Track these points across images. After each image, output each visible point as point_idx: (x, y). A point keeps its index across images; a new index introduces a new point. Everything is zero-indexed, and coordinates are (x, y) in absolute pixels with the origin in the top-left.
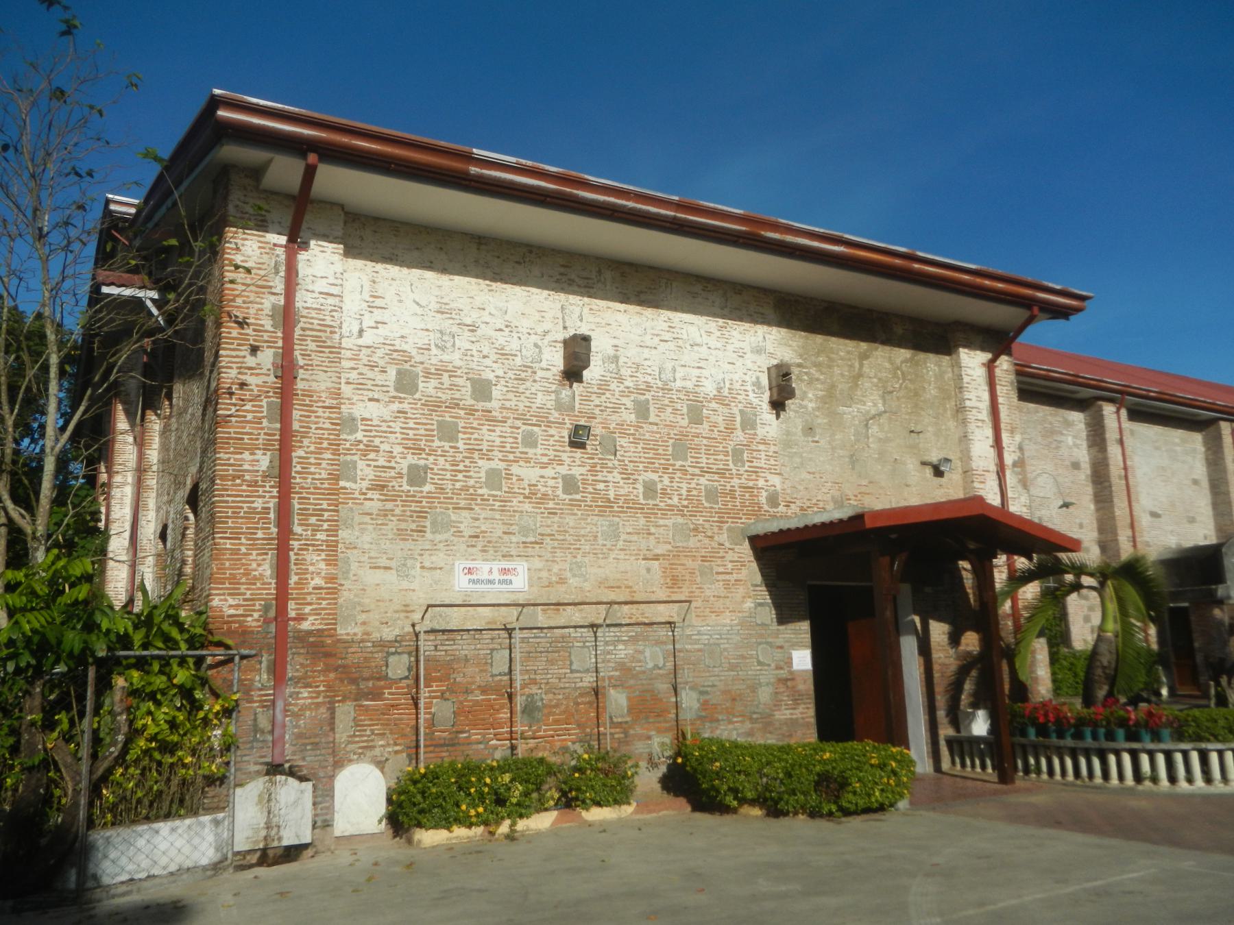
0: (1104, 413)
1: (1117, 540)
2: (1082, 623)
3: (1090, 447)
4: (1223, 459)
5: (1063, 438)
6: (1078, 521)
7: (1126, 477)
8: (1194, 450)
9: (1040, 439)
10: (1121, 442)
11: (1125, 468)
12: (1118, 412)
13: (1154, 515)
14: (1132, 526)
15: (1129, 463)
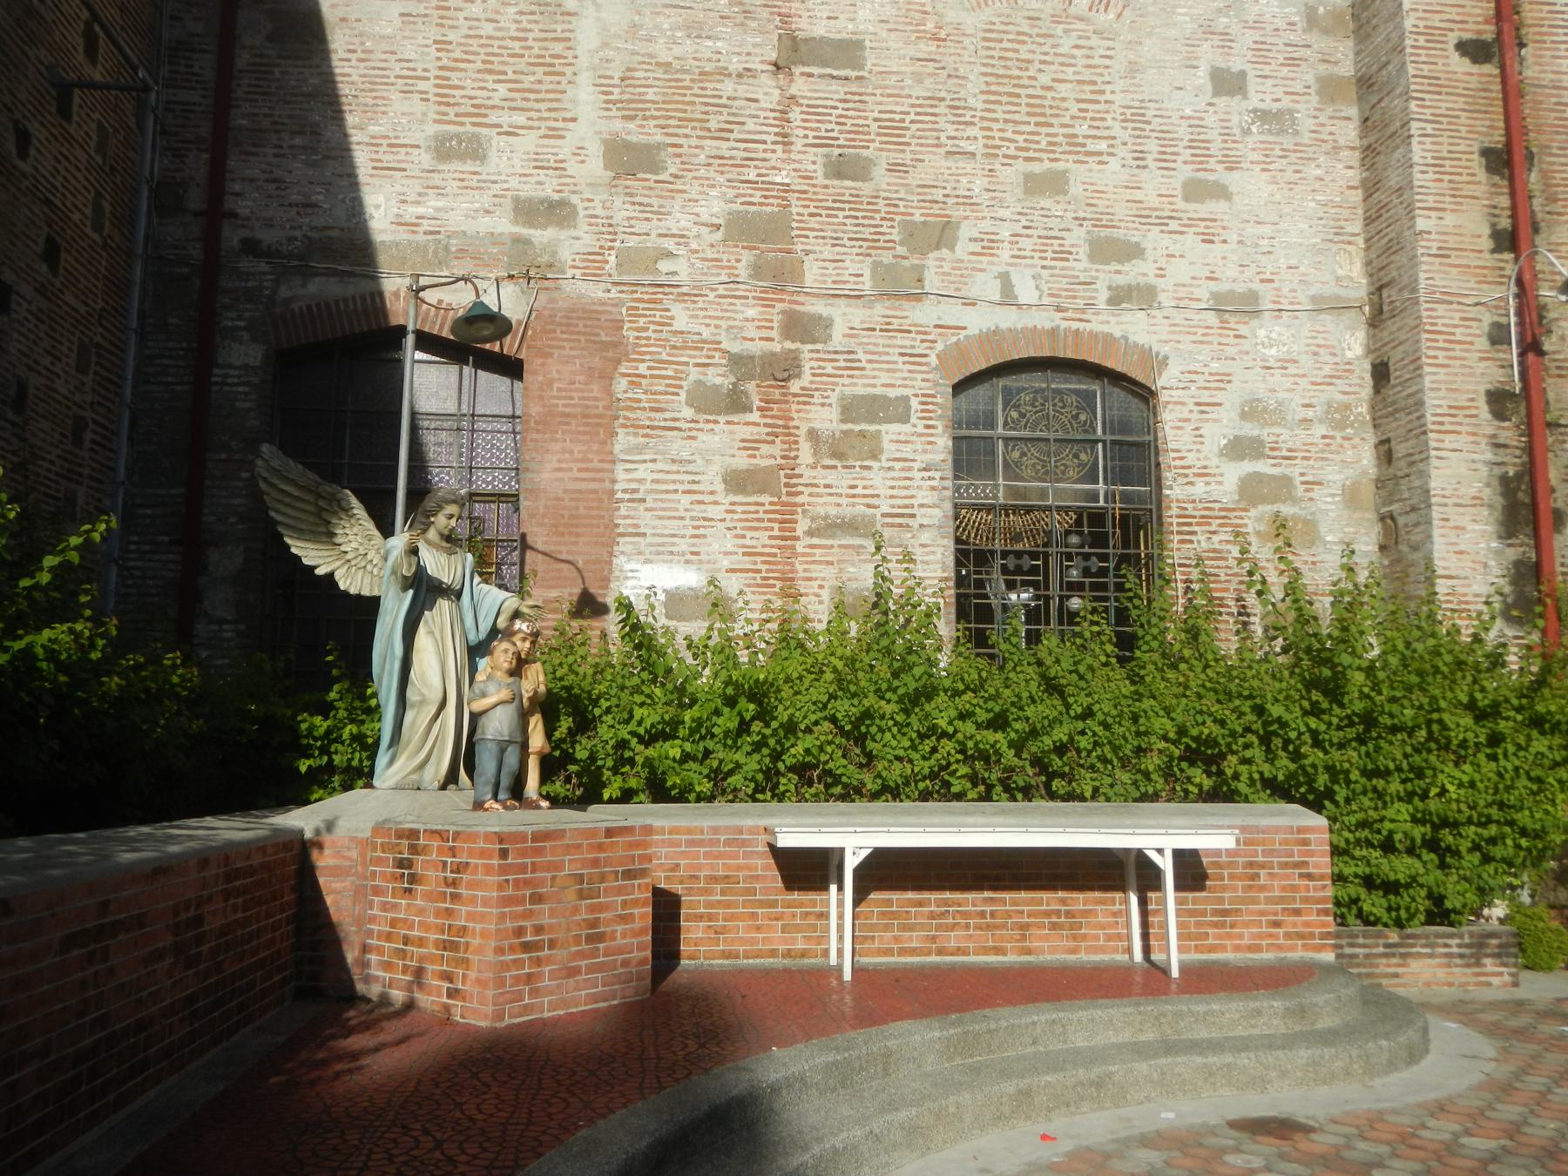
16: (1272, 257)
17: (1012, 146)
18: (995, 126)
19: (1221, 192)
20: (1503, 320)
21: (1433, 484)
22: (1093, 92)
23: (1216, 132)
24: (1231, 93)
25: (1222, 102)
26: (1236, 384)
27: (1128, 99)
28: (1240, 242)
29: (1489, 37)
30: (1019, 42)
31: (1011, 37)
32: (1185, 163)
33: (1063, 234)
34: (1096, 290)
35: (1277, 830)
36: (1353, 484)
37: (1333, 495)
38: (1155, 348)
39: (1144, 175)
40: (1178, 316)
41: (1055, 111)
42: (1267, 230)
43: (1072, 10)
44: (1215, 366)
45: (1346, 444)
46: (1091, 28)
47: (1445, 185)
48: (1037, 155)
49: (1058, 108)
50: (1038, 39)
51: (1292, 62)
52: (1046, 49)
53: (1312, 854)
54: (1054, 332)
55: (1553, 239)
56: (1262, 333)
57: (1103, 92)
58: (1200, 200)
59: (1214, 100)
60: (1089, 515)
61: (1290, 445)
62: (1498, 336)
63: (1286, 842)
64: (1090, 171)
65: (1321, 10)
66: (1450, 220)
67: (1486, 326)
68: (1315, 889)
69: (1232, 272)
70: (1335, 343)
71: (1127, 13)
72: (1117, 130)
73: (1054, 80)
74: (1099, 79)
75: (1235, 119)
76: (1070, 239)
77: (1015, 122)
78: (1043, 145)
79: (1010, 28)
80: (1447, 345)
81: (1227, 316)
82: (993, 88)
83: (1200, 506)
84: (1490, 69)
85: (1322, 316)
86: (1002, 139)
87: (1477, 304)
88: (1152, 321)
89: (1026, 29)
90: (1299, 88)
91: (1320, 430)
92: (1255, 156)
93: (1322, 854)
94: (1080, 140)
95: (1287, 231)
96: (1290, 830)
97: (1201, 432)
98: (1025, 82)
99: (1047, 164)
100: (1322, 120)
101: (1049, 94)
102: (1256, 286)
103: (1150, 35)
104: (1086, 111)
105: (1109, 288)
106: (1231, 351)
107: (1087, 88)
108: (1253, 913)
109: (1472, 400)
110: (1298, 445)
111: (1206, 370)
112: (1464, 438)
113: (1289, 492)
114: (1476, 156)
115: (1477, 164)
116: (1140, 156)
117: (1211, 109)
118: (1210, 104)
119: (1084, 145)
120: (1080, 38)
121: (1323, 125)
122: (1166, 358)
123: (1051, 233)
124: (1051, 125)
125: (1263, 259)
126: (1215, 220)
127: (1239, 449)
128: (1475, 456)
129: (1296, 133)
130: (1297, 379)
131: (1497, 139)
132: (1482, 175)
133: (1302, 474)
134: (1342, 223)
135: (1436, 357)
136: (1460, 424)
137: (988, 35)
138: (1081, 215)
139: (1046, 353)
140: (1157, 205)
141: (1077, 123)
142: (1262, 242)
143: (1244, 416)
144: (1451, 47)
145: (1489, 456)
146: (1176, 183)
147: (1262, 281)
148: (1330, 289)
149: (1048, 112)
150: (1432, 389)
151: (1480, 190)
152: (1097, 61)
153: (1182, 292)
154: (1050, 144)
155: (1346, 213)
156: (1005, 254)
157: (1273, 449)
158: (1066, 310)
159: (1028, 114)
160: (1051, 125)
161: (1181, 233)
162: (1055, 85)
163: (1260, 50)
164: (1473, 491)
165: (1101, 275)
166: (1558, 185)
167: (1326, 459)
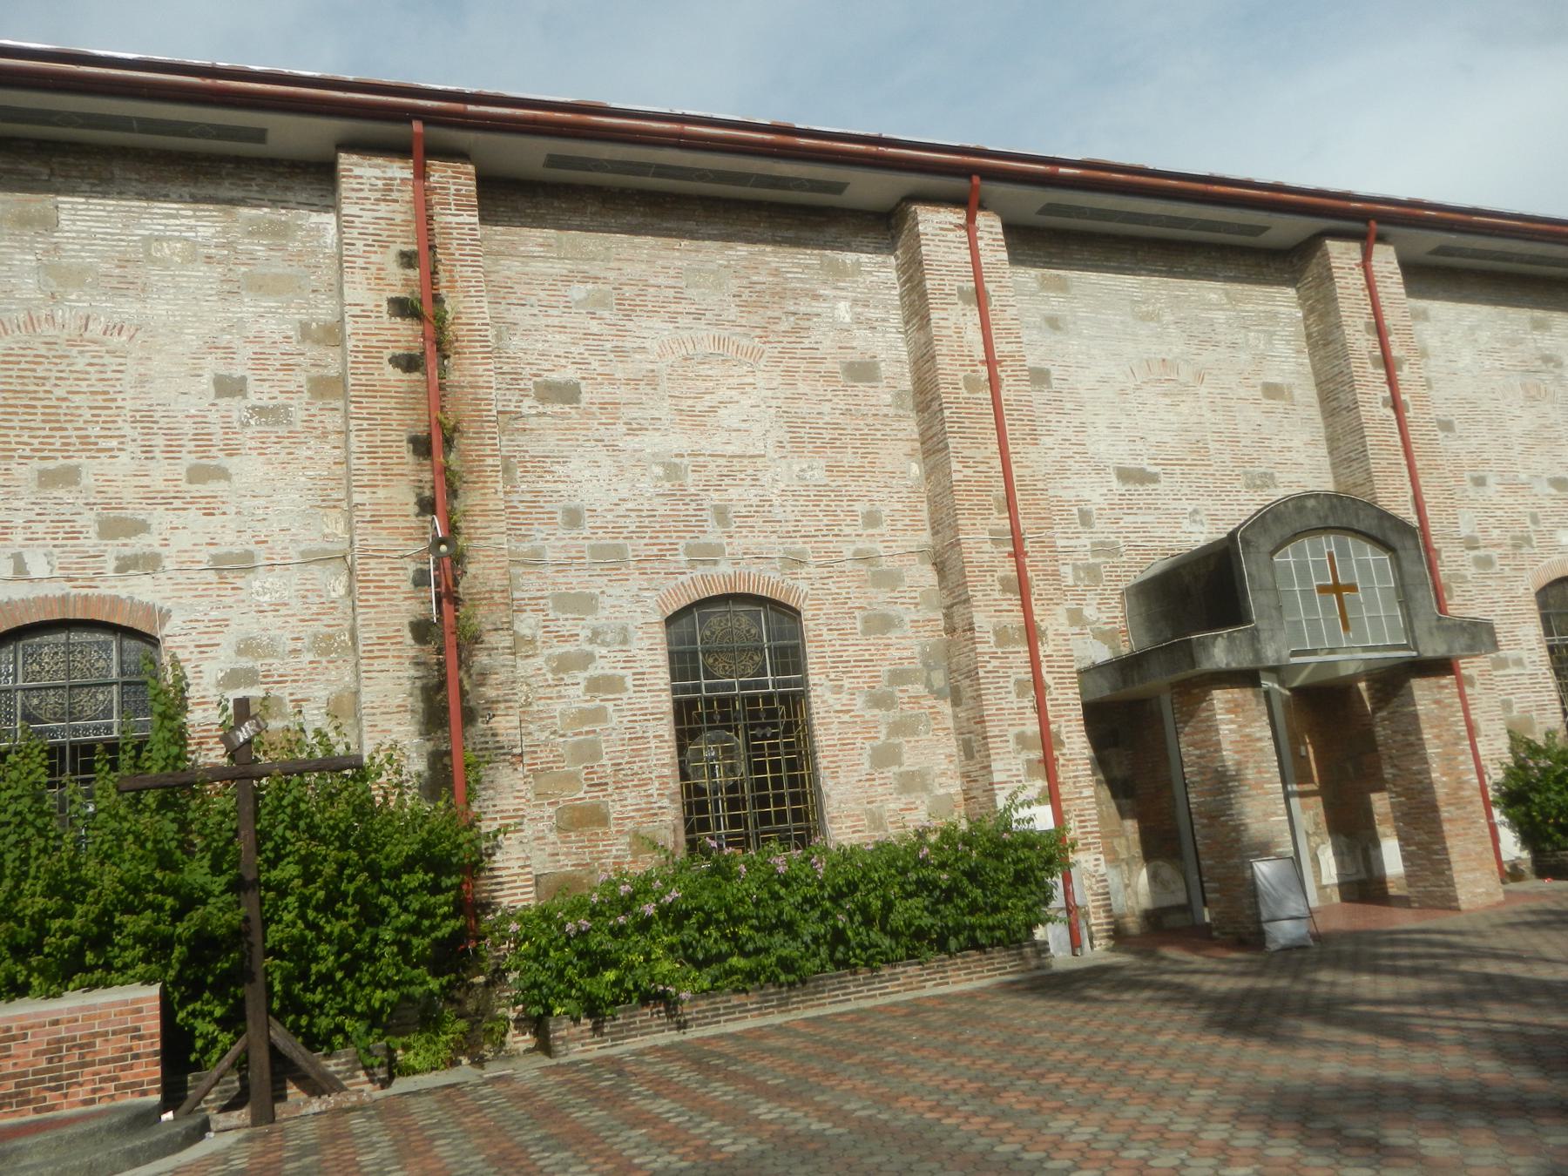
0: (921, 228)
1: (958, 543)
2: (867, 765)
3: (907, 323)
4: (1339, 326)
5: (817, 307)
6: (860, 507)
7: (994, 383)
8: (1273, 317)
9: (733, 312)
10: (980, 297)
11: (991, 361)
12: (970, 226)
13: (1125, 475)
14: (1010, 503)
15: (1001, 347)
16: (266, 523)
17: (28, 448)
18: (12, 433)
19: (222, 474)
20: (425, 567)
21: (363, 700)
22: (105, 400)
23: (218, 427)
24: (232, 394)
25: (223, 402)
26: (233, 627)
27: (138, 404)
28: (238, 513)
29: (417, 352)
30: (36, 363)
31: (28, 359)
32: (190, 452)
33: (74, 517)
34: (105, 561)
35: (113, 1004)
36: (337, 698)
37: (319, 708)
38: (159, 604)
39: (151, 464)
40: (181, 577)
41: (69, 418)
42: (262, 502)
43: (87, 335)
44: (214, 614)
45: (331, 666)
46: (104, 349)
47: (378, 466)
48: (51, 454)
49: (72, 415)
50: (55, 360)
51: (287, 368)
52: (60, 367)
53: (143, 1019)
54: (64, 599)
55: (469, 502)
56: (256, 584)
57: (115, 400)
58: (203, 481)
59: (216, 401)
60: (82, 747)
61: (281, 671)
62: (420, 580)
63: (121, 1013)
64: (101, 464)
65: (314, 325)
66: (381, 493)
67: (411, 573)
68: (145, 1046)
69: (229, 537)
70: (323, 587)
71: (139, 335)
72: (127, 429)
73: (68, 392)
74: (111, 390)
75: (235, 415)
76: (80, 521)
77: (31, 429)
78: (58, 446)
79: (28, 352)
80: (377, 590)
81: (225, 573)
82: (11, 402)
83: (199, 729)
84: (416, 376)
85: (311, 567)
86: (17, 443)
87: (402, 557)
88: (157, 582)
89: (43, 351)
90: (293, 387)
91: (310, 657)
92: (253, 444)
93: (153, 1018)
94: (93, 440)
95: (279, 502)
96: (125, 1003)
97: (201, 668)
98: (41, 395)
99: (61, 461)
100: (313, 411)
101: (64, 404)
102: (252, 547)
103: (159, 352)
104: (99, 416)
105: (117, 558)
106: (227, 601)
107: (100, 397)
108: (88, 1074)
109: (398, 630)
110: (289, 671)
111: (206, 618)
112: (391, 660)
113: (280, 709)
114: (405, 443)
115: (406, 449)
116: (148, 451)
117: (214, 408)
118: (214, 405)
119: (96, 444)
120: (94, 357)
121: (314, 415)
122: (169, 611)
123: (63, 518)
124: (66, 429)
125: (259, 525)
126: (215, 497)
127: (234, 678)
128: (400, 674)
129: (290, 423)
130: (288, 619)
131: (421, 430)
132: (409, 458)
133: (291, 694)
134: (329, 492)
135: (367, 600)
136: (388, 650)
137: (7, 359)
138: (92, 500)
139: (57, 616)
140: (163, 488)
141: (89, 426)
142: (257, 512)
143: (239, 652)
144: (385, 361)
145: (412, 673)
146: (183, 471)
147: (257, 543)
148: (318, 544)
149: (63, 418)
150: (363, 626)
151: (406, 469)
152: (109, 375)
153: (185, 557)
154: (64, 444)
155: (332, 484)
156: (18, 538)
157: (265, 676)
158: (76, 579)
159: (43, 421)
160: (66, 429)
161: (184, 509)
162: (70, 396)
163: (260, 359)
164: (398, 701)
165: (109, 549)
166: (474, 461)
167: (313, 680)
